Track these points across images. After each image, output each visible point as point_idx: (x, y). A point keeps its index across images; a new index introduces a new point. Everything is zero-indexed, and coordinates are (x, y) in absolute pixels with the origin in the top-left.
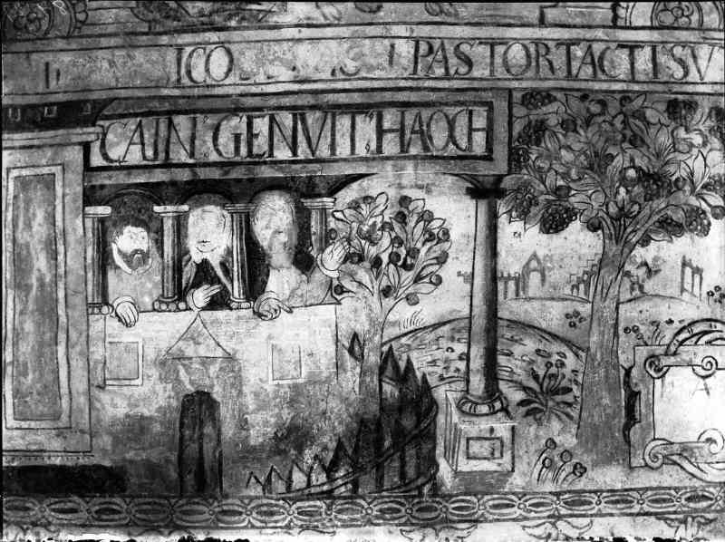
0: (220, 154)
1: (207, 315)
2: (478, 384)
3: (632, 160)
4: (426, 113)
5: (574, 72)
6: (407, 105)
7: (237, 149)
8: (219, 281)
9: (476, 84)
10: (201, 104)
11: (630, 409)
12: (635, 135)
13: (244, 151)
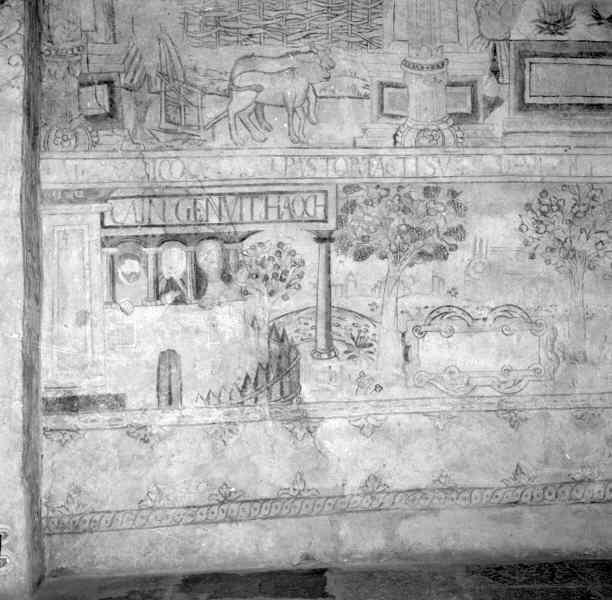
0: (179, 219)
1: (173, 307)
2: (322, 343)
3: (404, 220)
4: (292, 197)
5: (372, 173)
6: (281, 193)
7: (188, 217)
8: (180, 289)
9: (319, 181)
10: (168, 192)
11: (406, 356)
12: (405, 207)
13: (192, 218)
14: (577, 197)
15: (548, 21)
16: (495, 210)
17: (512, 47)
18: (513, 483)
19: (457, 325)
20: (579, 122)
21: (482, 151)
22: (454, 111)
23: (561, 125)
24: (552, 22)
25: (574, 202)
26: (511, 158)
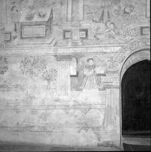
14: (34, 59)
15: (28, 17)
16: (15, 62)
17: (20, 24)
18: (16, 126)
19: (6, 89)
20: (35, 41)
21: (12, 49)
22: (6, 40)
23: (31, 42)
24: (29, 17)
25: (33, 60)
26: (19, 50)
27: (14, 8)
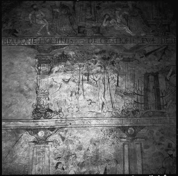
27: (59, 165)
